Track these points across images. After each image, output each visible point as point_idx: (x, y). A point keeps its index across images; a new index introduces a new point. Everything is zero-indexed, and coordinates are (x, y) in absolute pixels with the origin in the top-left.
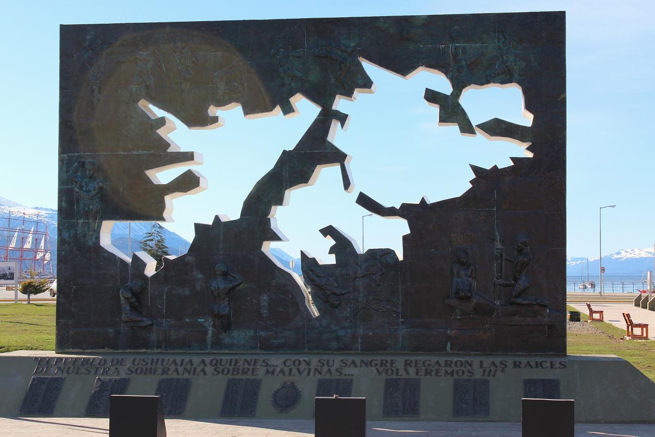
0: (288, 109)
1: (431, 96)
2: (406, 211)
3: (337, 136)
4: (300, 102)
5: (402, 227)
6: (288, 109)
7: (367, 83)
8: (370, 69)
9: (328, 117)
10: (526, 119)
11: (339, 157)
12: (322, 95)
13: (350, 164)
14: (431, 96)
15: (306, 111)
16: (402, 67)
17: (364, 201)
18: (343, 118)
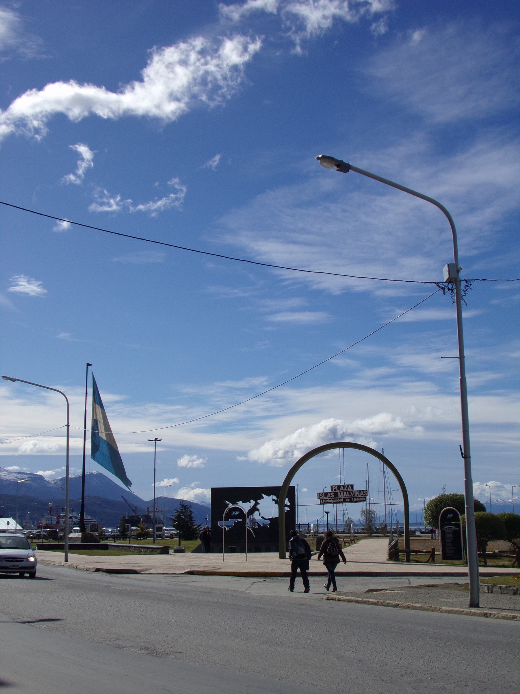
0: (250, 502)
1: (273, 500)
2: (269, 519)
3: (258, 507)
4: (252, 501)
5: (269, 522)
6: (250, 502)
7: (263, 498)
8: (264, 496)
9: (257, 503)
10: (289, 504)
11: (258, 510)
12: (256, 500)
13: (260, 511)
14: (273, 500)
15: (253, 502)
16: (269, 495)
17: (262, 517)
18: (259, 504)
